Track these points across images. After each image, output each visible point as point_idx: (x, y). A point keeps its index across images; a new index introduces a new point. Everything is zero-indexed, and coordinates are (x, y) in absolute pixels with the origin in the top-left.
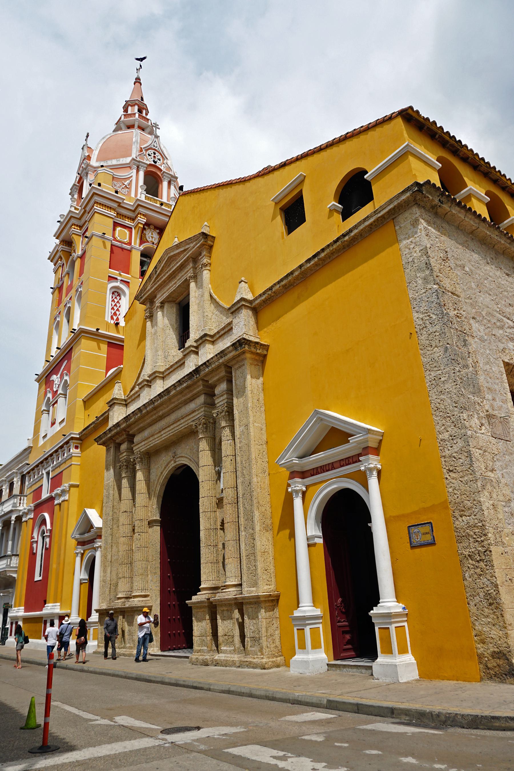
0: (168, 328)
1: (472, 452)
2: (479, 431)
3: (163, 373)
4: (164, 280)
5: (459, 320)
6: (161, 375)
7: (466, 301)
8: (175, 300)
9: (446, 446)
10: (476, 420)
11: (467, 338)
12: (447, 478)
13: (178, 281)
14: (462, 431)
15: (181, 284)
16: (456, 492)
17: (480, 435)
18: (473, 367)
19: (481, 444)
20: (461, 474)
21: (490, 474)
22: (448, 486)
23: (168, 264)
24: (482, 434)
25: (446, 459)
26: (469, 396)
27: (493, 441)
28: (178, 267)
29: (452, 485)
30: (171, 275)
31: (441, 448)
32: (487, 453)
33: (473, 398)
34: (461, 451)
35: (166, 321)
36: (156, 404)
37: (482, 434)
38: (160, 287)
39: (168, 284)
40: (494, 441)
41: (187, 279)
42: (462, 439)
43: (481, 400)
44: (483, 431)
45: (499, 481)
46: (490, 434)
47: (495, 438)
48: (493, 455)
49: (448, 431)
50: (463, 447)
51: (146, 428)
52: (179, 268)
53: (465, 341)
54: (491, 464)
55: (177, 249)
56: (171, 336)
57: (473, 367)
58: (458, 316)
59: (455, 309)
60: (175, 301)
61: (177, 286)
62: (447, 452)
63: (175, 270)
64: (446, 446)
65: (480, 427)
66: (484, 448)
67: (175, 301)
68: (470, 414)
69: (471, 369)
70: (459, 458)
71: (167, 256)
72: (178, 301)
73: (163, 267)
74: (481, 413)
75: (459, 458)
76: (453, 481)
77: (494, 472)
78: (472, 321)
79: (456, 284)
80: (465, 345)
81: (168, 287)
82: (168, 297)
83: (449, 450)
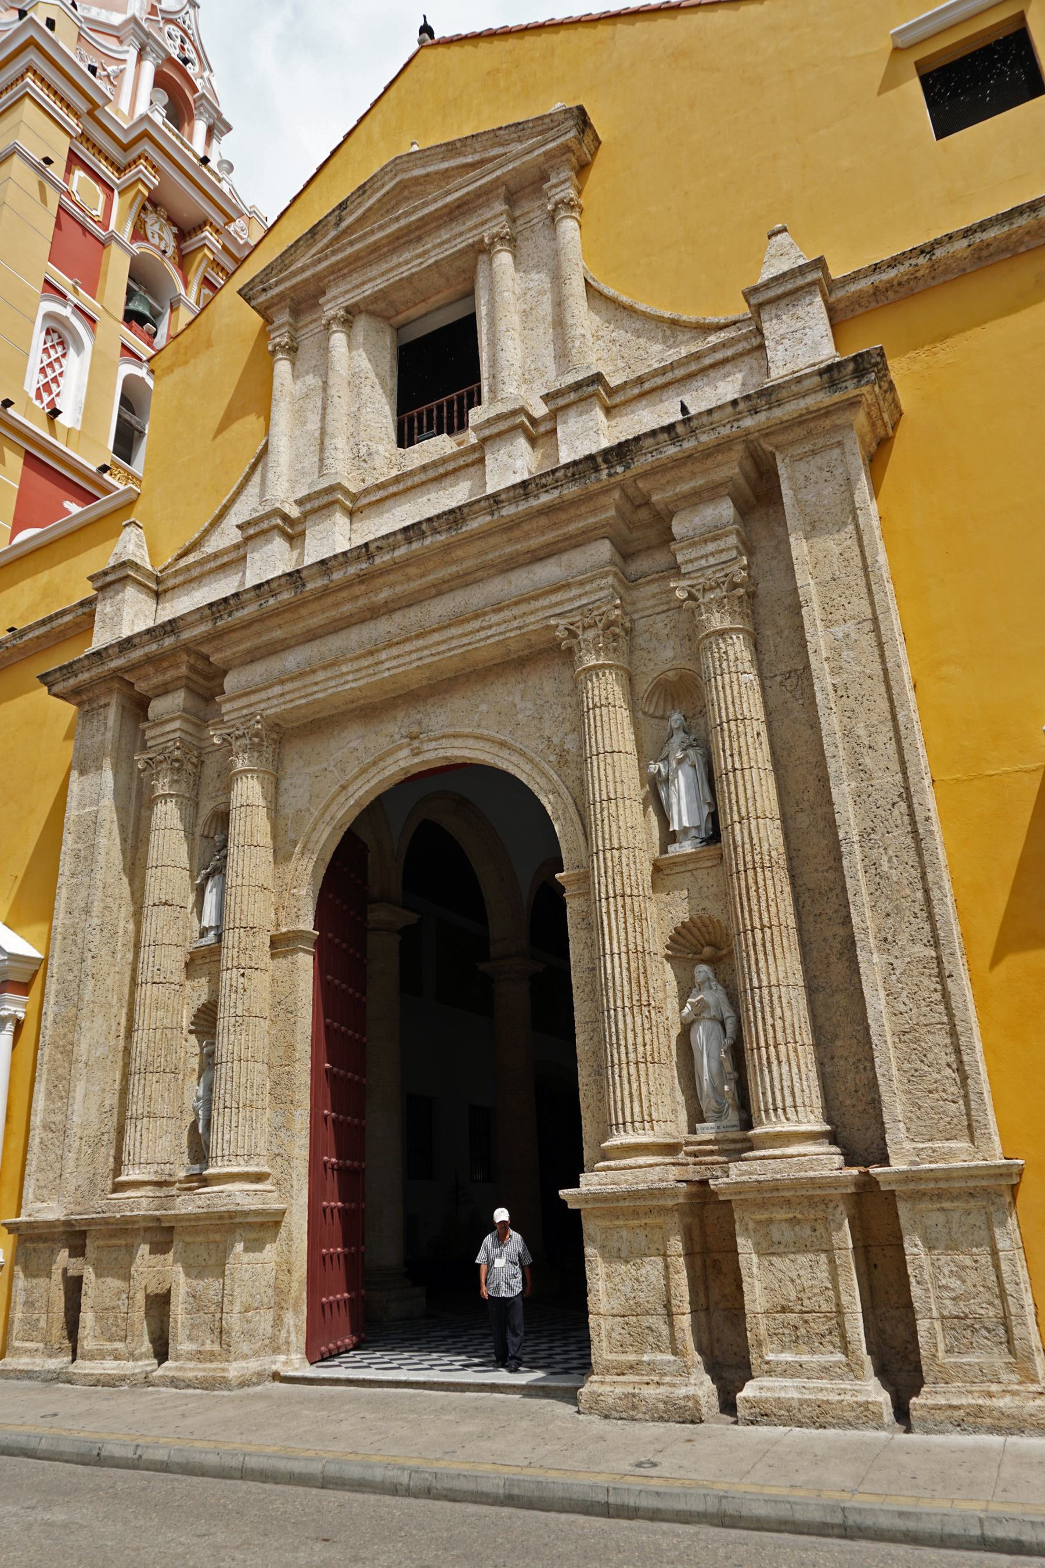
0: (369, 382)
3: (354, 497)
4: (375, 242)
6: (348, 503)
8: (392, 312)
13: (434, 247)
15: (443, 259)
23: (389, 207)
28: (445, 206)
30: (409, 229)
35: (363, 361)
36: (337, 576)
38: (350, 264)
39: (383, 257)
41: (482, 240)
51: (292, 647)
52: (446, 210)
55: (444, 159)
56: (377, 406)
60: (389, 318)
61: (430, 261)
63: (431, 213)
67: (389, 318)
71: (391, 179)
72: (401, 318)
73: (370, 209)
81: (385, 266)
82: (375, 297)
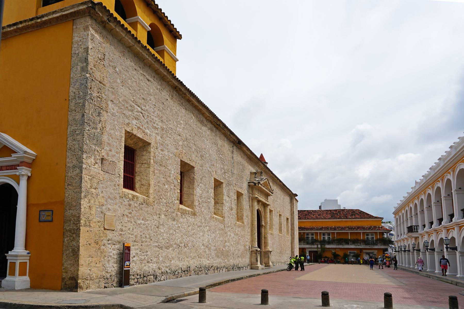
1: (83, 177)
2: (92, 166)
5: (99, 99)
7: (109, 89)
9: (70, 171)
10: (93, 160)
11: (101, 112)
12: (66, 188)
14: (80, 164)
16: (69, 196)
17: (93, 168)
18: (100, 129)
19: (91, 173)
20: (74, 187)
21: (93, 191)
22: (66, 193)
24: (95, 168)
25: (69, 178)
26: (91, 146)
27: (101, 173)
29: (68, 192)
31: (67, 171)
32: (94, 179)
33: (94, 147)
34: (77, 175)
37: (95, 168)
40: (102, 173)
42: (80, 169)
43: (100, 149)
44: (95, 167)
45: (98, 195)
46: (100, 169)
47: (104, 172)
48: (99, 181)
49: (73, 163)
50: (78, 173)
53: (99, 113)
54: (96, 185)
57: (100, 129)
58: (99, 97)
59: (98, 92)
62: (70, 174)
64: (70, 171)
65: (94, 164)
66: (93, 176)
68: (89, 156)
69: (98, 130)
70: (76, 179)
74: (97, 157)
75: (76, 179)
76: (70, 190)
77: (96, 189)
78: (110, 103)
79: (105, 77)
80: (99, 116)
83: (71, 173)
